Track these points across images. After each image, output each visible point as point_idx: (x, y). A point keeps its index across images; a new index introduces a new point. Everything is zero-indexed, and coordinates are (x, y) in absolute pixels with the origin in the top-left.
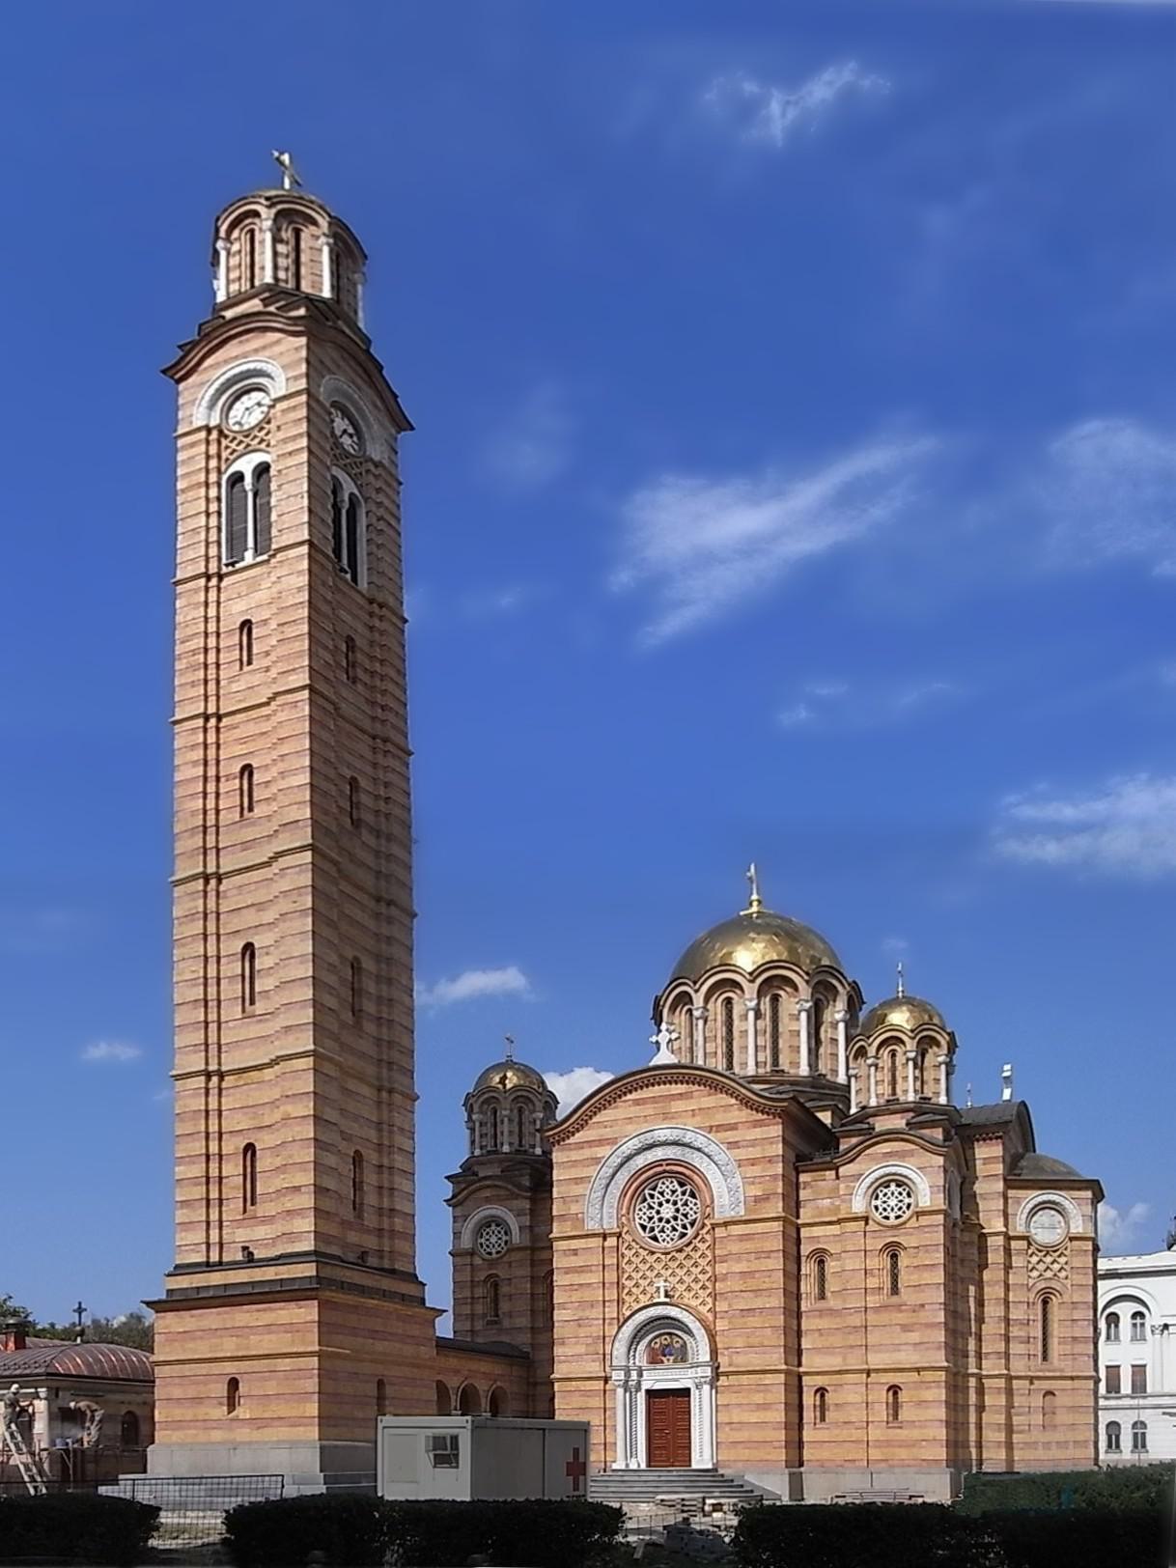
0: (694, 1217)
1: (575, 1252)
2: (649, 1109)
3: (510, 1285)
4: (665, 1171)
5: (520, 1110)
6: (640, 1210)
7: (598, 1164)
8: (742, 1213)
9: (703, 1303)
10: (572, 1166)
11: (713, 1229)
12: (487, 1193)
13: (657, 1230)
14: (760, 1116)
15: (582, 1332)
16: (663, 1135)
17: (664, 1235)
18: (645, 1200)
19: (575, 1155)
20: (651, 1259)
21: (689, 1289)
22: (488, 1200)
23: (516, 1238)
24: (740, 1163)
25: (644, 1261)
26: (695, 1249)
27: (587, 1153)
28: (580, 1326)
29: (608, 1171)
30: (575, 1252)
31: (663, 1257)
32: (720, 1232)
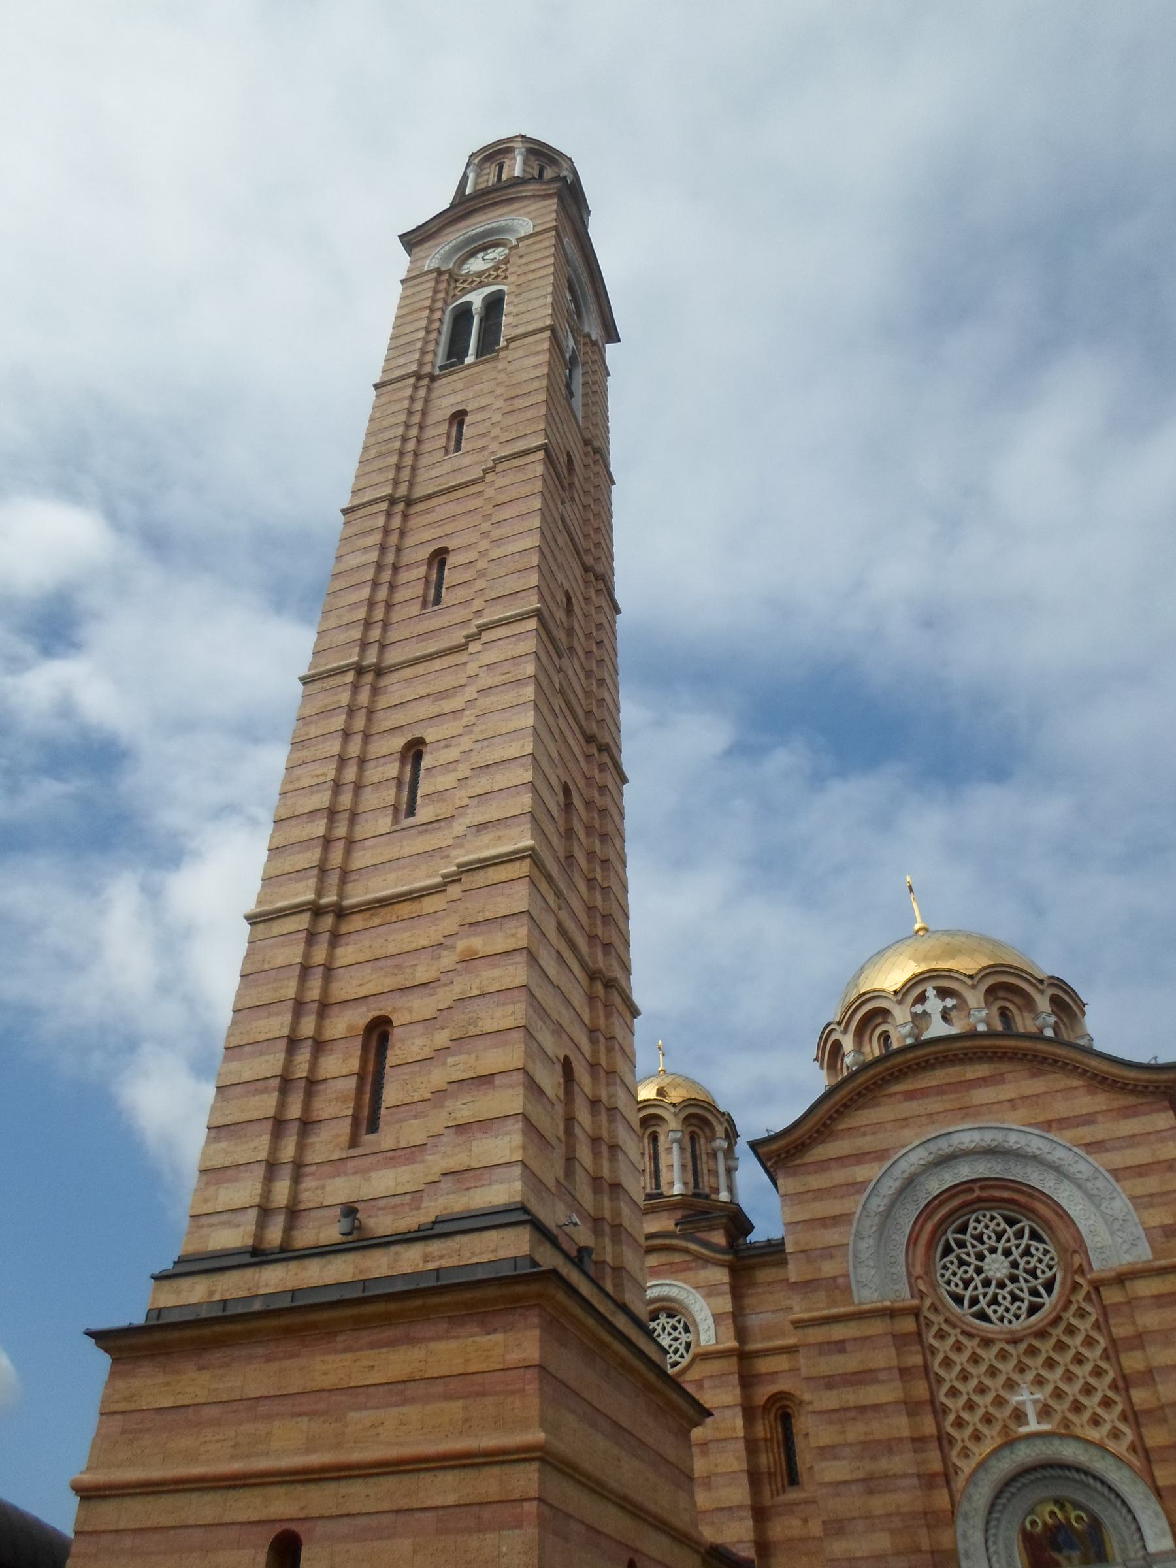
0: (1049, 1274)
1: (840, 1346)
2: (934, 1105)
4: (980, 1200)
5: (693, 1138)
6: (945, 1267)
7: (859, 1192)
8: (1150, 1256)
9: (1116, 1434)
10: (815, 1199)
11: (1097, 1289)
13: (983, 1302)
14: (1131, 1100)
15: (878, 1504)
16: (968, 1139)
17: (1001, 1310)
18: (948, 1250)
19: (816, 1181)
21: (1077, 1407)
23: (708, 1335)
24: (1117, 1173)
25: (975, 1359)
26: (1071, 1331)
27: (839, 1176)
28: (871, 1492)
29: (879, 1204)
30: (840, 1346)
31: (1009, 1348)
32: (1112, 1296)
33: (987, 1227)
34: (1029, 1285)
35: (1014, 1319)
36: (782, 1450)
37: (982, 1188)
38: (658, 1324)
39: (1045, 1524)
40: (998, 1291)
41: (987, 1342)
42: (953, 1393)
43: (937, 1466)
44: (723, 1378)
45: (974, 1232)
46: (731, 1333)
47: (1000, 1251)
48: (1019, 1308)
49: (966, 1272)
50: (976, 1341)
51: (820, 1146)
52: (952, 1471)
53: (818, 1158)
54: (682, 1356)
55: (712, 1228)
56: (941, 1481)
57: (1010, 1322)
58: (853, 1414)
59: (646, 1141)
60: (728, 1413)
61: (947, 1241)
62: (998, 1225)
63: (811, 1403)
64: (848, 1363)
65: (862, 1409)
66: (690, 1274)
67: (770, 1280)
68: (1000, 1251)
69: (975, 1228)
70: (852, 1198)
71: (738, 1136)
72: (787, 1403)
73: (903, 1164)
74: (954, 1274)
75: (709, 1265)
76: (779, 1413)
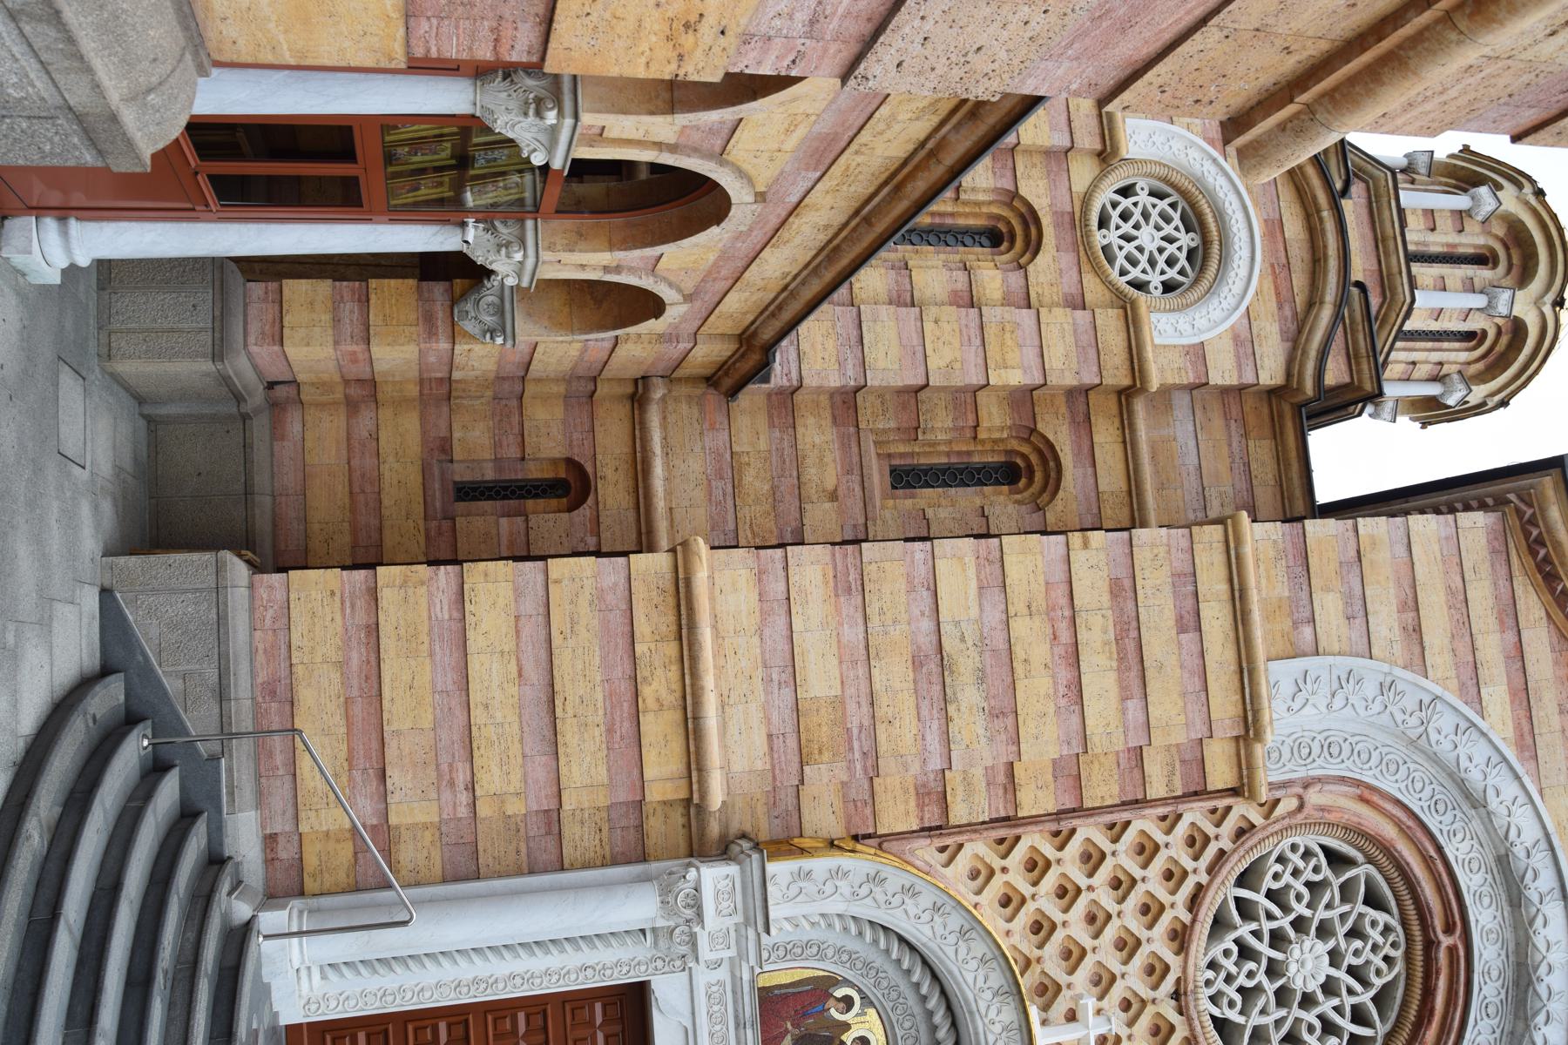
1: (1190, 622)
3: (1007, 301)
4: (1430, 945)
5: (1470, 337)
6: (1307, 854)
10: (1450, 590)
12: (1294, 228)
13: (1244, 930)
15: (893, 675)
17: (1229, 965)
18: (1337, 860)
19: (1482, 596)
20: (1157, 943)
22: (1275, 227)
27: (1492, 647)
28: (917, 663)
30: (1190, 622)
31: (1168, 985)
33: (1375, 948)
34: (1271, 1027)
35: (1212, 991)
36: (954, 460)
37: (1452, 950)
38: (1177, 229)
39: (846, 1027)
40: (1264, 963)
41: (1180, 938)
42: (1092, 859)
43: (959, 814)
44: (1092, 353)
45: (1367, 921)
46: (1172, 379)
47: (1333, 972)
48: (1231, 1004)
49: (1299, 898)
50: (1186, 917)
51: (1543, 614)
52: (949, 841)
53: (1521, 605)
54: (1123, 273)
55: (1351, 357)
56: (932, 817)
57: (1208, 983)
58: (1065, 636)
59: (1481, 240)
60: (1031, 354)
61: (1349, 862)
62: (1378, 973)
63: (1086, 545)
64: (1160, 641)
65: (1074, 656)
66: (1272, 305)
67: (1254, 466)
68: (1333, 972)
69: (1374, 924)
70: (1453, 673)
71: (1424, 426)
72: (1038, 476)
73: (1510, 790)
74: (1296, 873)
75: (1289, 344)
76: (1019, 461)
